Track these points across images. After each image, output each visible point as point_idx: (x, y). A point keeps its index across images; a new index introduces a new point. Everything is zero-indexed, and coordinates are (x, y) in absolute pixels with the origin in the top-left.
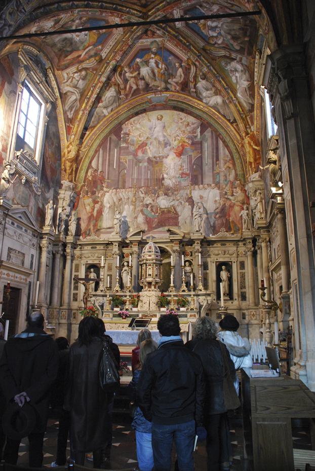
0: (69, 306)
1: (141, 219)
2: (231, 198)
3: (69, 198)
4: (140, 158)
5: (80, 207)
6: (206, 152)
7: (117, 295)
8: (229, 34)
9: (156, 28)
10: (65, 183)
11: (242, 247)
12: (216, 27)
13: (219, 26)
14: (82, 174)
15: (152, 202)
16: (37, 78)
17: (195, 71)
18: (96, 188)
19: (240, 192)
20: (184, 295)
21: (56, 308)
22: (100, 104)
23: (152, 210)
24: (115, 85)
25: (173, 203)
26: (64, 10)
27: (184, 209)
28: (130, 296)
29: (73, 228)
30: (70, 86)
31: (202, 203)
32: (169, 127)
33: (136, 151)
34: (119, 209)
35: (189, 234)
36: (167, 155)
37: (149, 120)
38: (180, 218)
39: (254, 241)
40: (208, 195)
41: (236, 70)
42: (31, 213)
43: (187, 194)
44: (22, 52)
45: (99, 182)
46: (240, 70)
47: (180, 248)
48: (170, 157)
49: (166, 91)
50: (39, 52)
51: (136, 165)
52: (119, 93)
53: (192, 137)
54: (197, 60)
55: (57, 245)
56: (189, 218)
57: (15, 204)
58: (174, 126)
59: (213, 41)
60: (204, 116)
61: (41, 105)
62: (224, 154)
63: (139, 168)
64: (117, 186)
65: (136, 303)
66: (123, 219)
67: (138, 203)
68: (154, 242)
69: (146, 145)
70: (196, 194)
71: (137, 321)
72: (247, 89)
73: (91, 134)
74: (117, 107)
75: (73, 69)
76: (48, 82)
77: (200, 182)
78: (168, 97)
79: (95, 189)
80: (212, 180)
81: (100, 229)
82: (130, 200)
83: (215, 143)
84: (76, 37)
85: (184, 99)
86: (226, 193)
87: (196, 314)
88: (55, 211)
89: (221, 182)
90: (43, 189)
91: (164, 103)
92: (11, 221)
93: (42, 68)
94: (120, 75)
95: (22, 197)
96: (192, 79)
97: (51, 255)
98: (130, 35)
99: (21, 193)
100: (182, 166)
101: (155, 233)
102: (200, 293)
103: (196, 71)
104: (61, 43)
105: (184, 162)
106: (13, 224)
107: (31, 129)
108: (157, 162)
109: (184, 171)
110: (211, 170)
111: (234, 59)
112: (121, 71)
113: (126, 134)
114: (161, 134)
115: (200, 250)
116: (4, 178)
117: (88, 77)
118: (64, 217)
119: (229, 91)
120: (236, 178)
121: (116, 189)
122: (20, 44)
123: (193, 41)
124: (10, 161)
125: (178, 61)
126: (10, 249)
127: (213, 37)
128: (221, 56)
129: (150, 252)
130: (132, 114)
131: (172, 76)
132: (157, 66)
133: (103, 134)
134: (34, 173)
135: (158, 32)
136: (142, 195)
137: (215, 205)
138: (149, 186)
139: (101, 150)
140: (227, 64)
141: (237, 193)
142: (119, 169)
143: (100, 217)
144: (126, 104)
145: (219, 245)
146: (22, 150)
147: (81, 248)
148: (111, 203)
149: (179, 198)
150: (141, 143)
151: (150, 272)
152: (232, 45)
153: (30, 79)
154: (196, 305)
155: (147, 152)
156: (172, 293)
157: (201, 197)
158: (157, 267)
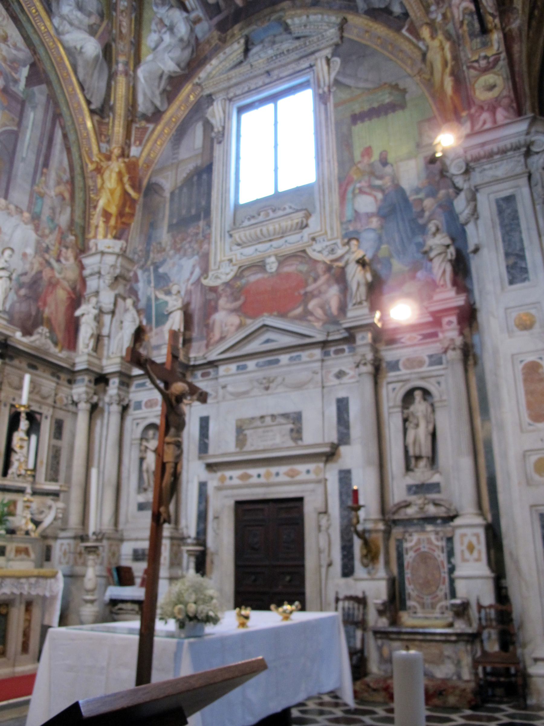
11: (65, 386)
19: (72, 260)
39: (101, 380)
41: (171, 29)
46: (179, 35)
62: (61, 163)
72: (165, 77)
83: (49, 125)
86: (47, 250)
89: (45, 217)
110: (30, 180)
141: (67, 259)
145: (24, 365)
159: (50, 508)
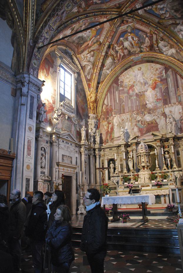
0: (101, 184)
1: (136, 129)
3: (94, 123)
4: (131, 94)
5: (101, 127)
6: (170, 84)
7: (125, 175)
8: (172, 9)
9: (128, 18)
10: (91, 115)
12: (164, 7)
13: (165, 6)
14: (100, 109)
15: (141, 119)
16: (67, 61)
17: (156, 37)
18: (109, 115)
20: (166, 172)
21: (93, 186)
22: (105, 68)
23: (142, 123)
24: (111, 55)
25: (153, 118)
26: (74, 23)
27: (161, 120)
28: (133, 175)
29: (98, 139)
30: (86, 62)
31: (171, 115)
33: (129, 90)
34: (123, 126)
35: (165, 135)
37: (133, 71)
38: (159, 126)
40: (175, 109)
42: (73, 135)
43: (162, 111)
44: (57, 50)
45: (110, 112)
47: (161, 144)
48: (149, 91)
49: (141, 52)
50: (66, 48)
51: (129, 99)
52: (114, 59)
54: (155, 31)
55: (90, 150)
56: (165, 125)
57: (63, 131)
58: (149, 72)
59: (163, 16)
60: (166, 62)
61: (71, 75)
64: (120, 113)
65: (137, 179)
66: (125, 131)
67: (133, 121)
68: (144, 142)
69: (134, 86)
70: (167, 110)
71: (133, 190)
73: (102, 86)
74: (114, 68)
75: (86, 52)
76: (74, 62)
79: (108, 116)
80: (176, 101)
81: (113, 138)
82: (128, 119)
83: (175, 77)
84: (84, 34)
85: (152, 55)
87: (174, 183)
88: (87, 132)
90: (79, 120)
91: (141, 60)
92: (62, 140)
93: (69, 55)
94: (113, 49)
95: (67, 126)
96: (155, 42)
97: (88, 156)
98: (114, 26)
99: (66, 124)
100: (156, 95)
101: (145, 137)
102: (175, 170)
103: (157, 37)
104: (77, 40)
105: (158, 92)
106: (63, 141)
107: (68, 89)
108: (141, 95)
109: (158, 97)
110: (175, 95)
111: (178, 24)
112: (113, 47)
114: (141, 78)
115: (173, 144)
116: (55, 118)
117: (95, 55)
118: (92, 134)
119: (179, 44)
122: (55, 46)
123: (151, 20)
124: (58, 108)
125: (145, 34)
126: (63, 156)
127: (163, 14)
128: (170, 24)
129: (142, 148)
130: (123, 70)
131: (143, 43)
132: (133, 40)
133: (108, 85)
134: (72, 112)
135: (129, 20)
136: (135, 116)
137: (180, 115)
138: (138, 109)
140: (174, 28)
146: (63, 101)
147: (104, 150)
148: (118, 123)
149: (157, 114)
150: (130, 85)
151: (143, 160)
152: (176, 15)
153: (64, 63)
154: (173, 177)
155: (135, 90)
156: (157, 171)
157: (171, 112)
158: (147, 157)
159: (178, 174)
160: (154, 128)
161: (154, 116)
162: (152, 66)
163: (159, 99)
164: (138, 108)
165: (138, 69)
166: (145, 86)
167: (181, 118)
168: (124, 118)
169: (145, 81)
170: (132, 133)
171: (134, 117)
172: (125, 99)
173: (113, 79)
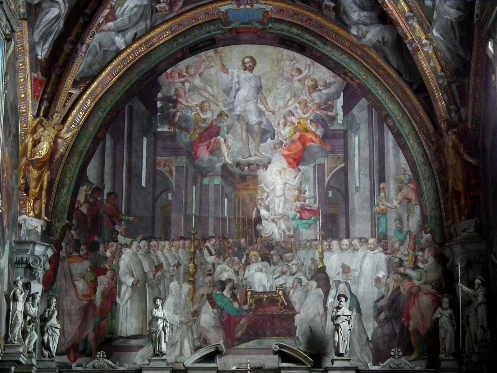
1: (207, 316)
2: (413, 274)
4: (204, 166)
18: (100, 235)
19: (431, 260)
23: (234, 296)
25: (281, 281)
31: (347, 284)
32: (270, 90)
36: (266, 161)
38: (297, 317)
53: (323, 120)
58: (282, 87)
62: (398, 165)
63: (203, 190)
70: (333, 261)
77: (343, 233)
78: (266, 12)
79: (96, 238)
82: (182, 269)
83: (376, 137)
86: (401, 263)
89: (391, 233)
105: (307, 180)
108: (243, 178)
109: (307, 202)
110: (367, 205)
113: (168, 100)
114: (251, 107)
120: (423, 227)
121: (148, 239)
130: (183, 48)
133: (112, 96)
136: (211, 259)
137: (376, 290)
139: (108, 137)
141: (425, 262)
142: (154, 189)
143: (111, 310)
144: (170, 23)
149: (294, 269)
155: (219, 149)
160: (277, 323)
161: (284, 276)
162: (297, 66)
163: (309, 210)
164: (223, 228)
165: (244, 64)
166: (261, 142)
167: (378, 300)
168: (166, 258)
169: (265, 122)
170: (191, 327)
171: (207, 263)
172: (177, 180)
173: (134, 77)
